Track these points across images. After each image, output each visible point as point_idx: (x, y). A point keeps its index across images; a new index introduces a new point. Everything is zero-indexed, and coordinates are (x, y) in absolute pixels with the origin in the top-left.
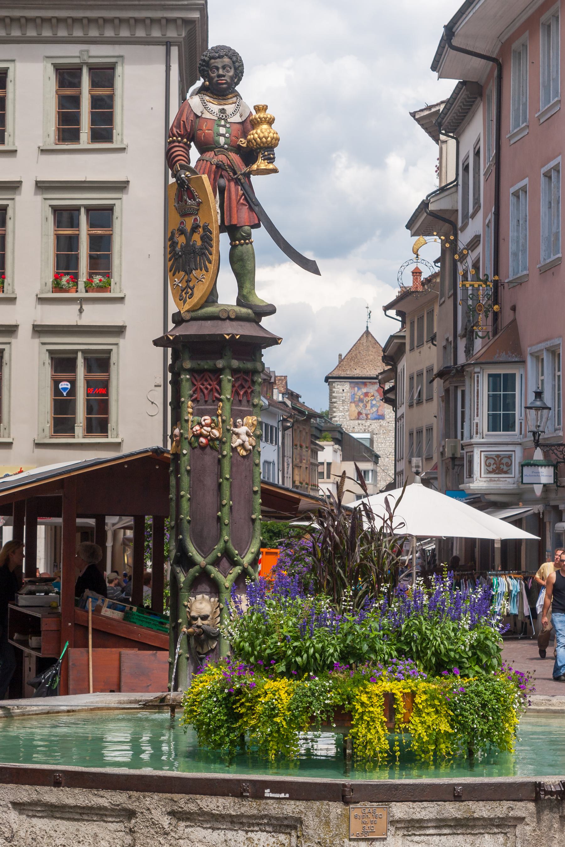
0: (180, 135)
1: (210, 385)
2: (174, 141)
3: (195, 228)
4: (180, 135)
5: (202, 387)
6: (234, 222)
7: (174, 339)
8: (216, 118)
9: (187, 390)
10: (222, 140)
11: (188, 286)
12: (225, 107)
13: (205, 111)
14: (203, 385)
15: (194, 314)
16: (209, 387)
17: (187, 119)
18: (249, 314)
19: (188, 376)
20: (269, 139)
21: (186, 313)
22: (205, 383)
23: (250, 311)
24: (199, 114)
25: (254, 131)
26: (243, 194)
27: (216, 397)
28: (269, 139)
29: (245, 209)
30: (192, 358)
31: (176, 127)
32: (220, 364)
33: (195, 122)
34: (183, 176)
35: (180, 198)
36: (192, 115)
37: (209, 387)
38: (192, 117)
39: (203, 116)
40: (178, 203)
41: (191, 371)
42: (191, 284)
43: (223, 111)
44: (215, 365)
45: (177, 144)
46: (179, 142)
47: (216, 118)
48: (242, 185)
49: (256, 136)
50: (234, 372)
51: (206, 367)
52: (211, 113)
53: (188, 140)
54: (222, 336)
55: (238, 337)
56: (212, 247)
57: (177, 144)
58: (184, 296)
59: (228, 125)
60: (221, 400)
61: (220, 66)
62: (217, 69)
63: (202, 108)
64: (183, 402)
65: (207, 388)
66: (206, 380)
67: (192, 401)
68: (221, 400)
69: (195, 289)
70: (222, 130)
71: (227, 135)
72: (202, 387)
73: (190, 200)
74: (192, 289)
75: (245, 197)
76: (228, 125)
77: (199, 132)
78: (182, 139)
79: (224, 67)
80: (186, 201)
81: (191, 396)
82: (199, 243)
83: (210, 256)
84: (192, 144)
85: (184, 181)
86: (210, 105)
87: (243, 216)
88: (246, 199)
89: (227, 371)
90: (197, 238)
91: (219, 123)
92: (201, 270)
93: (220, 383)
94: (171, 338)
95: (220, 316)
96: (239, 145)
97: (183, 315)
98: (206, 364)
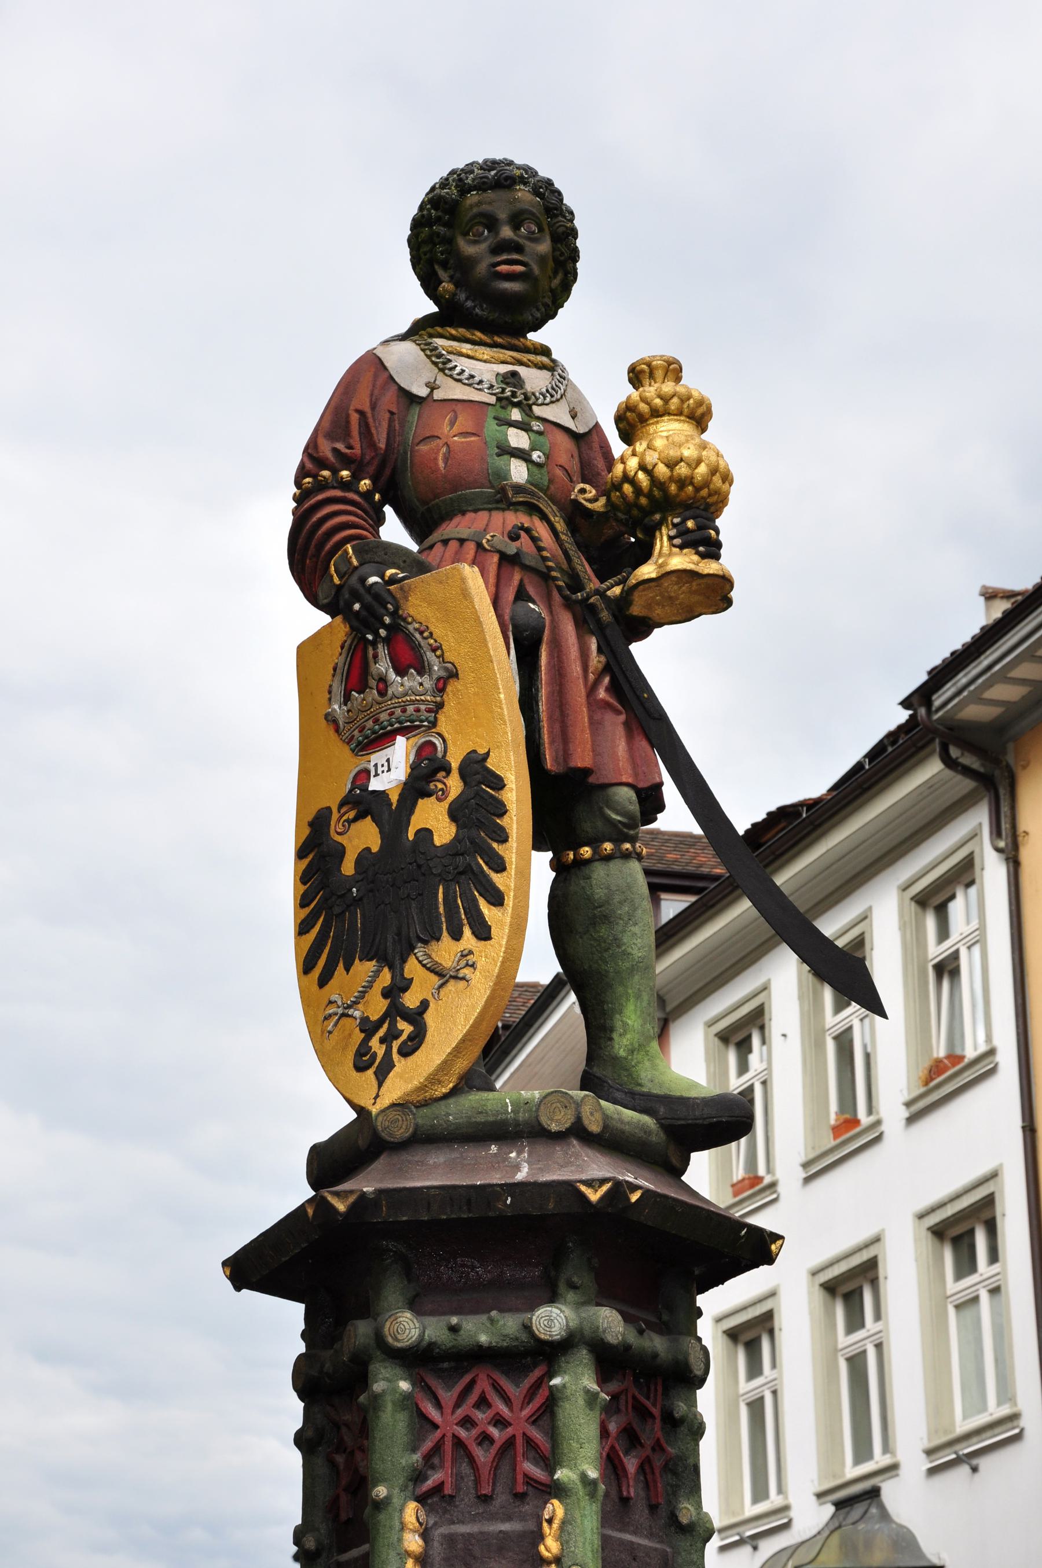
0: (346, 461)
1: (499, 1422)
2: (321, 486)
3: (422, 780)
4: (346, 461)
5: (462, 1433)
6: (582, 759)
7: (352, 1208)
8: (492, 400)
9: (394, 1451)
10: (518, 472)
11: (396, 1011)
12: (522, 370)
13: (441, 379)
14: (467, 1422)
15: (425, 1117)
16: (494, 1432)
17: (373, 407)
18: (648, 1132)
19: (404, 1385)
20: (702, 469)
21: (392, 1114)
22: (480, 1416)
23: (646, 1119)
24: (422, 392)
25: (640, 447)
26: (607, 669)
27: (529, 1480)
28: (702, 469)
29: (615, 725)
30: (415, 1305)
31: (331, 436)
32: (552, 1320)
33: (403, 423)
34: (373, 579)
35: (356, 675)
36: (391, 394)
37: (494, 1432)
38: (389, 400)
39: (438, 395)
40: (347, 698)
41: (418, 1359)
42: (411, 1000)
43: (512, 379)
44: (527, 1328)
45: (338, 493)
46: (345, 486)
47: (492, 400)
48: (600, 631)
49: (651, 458)
50: (609, 1360)
51: (483, 1339)
52: (471, 381)
53: (375, 488)
54: (569, 1189)
55: (634, 1197)
56: (504, 839)
57: (338, 493)
58: (379, 1050)
59: (536, 426)
60: (557, 1490)
61: (503, 216)
62: (491, 223)
63: (429, 372)
64: (380, 1505)
65: (485, 1439)
66: (483, 1402)
67: (421, 1499)
68: (557, 1490)
69: (429, 1017)
70: (518, 439)
71: (536, 456)
72: (462, 1433)
73: (401, 672)
74: (417, 1017)
75: (614, 682)
76: (536, 426)
77: (423, 448)
78: (356, 477)
79: (516, 220)
80: (383, 680)
81: (417, 1476)
82: (444, 832)
83: (497, 878)
84: (388, 510)
85: (377, 597)
86: (461, 364)
87: (609, 750)
88: (615, 688)
89: (584, 1355)
90: (434, 819)
91: (502, 414)
92: (457, 936)
93: (548, 1409)
94: (341, 1207)
95: (544, 1120)
96: (576, 502)
97: (380, 1124)
98: (481, 1330)
